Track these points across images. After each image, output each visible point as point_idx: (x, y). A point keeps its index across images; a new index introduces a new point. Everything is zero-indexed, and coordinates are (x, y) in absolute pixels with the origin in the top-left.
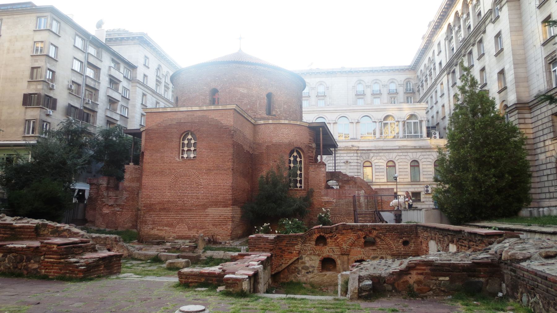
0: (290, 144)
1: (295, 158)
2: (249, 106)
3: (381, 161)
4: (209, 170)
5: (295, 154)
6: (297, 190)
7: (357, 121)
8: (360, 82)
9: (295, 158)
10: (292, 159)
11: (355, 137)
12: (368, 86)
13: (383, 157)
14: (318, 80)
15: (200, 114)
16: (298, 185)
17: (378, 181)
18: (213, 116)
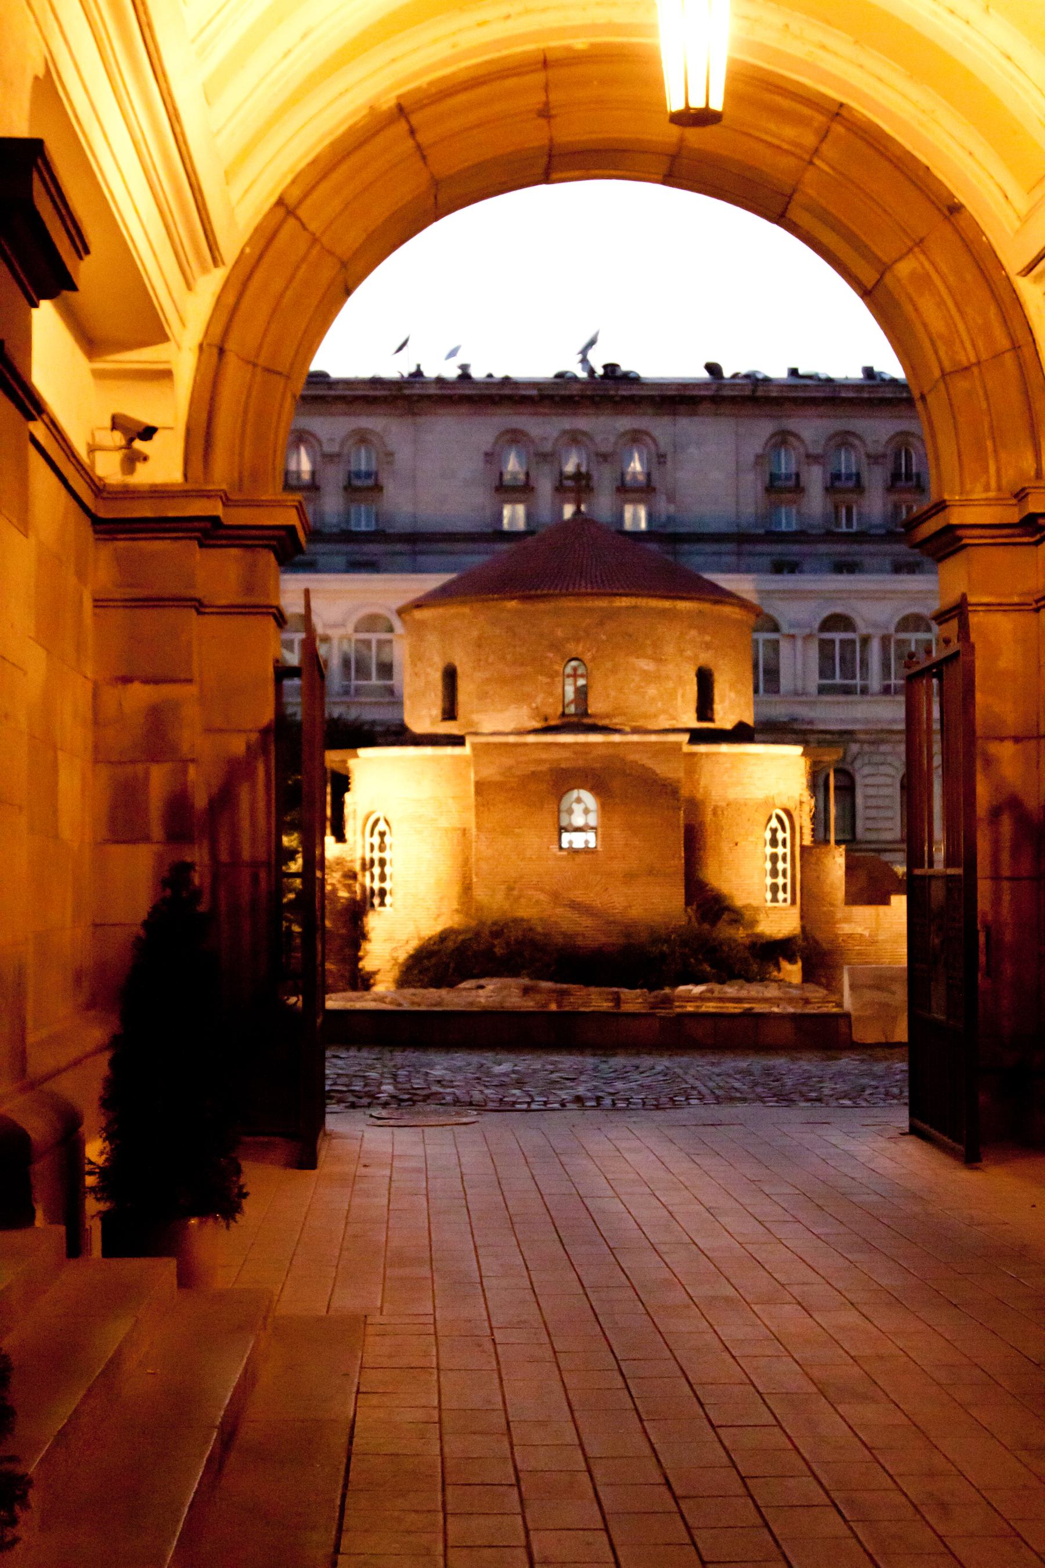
0: (768, 803)
1: (774, 831)
2: (660, 704)
3: (883, 769)
4: (630, 877)
5: (774, 823)
6: (781, 909)
7: (807, 631)
8: (782, 439)
9: (774, 831)
10: (768, 835)
11: (800, 684)
12: (812, 458)
13: (889, 759)
14: (625, 423)
15: (602, 751)
16: (781, 895)
17: (873, 836)
18: (632, 757)
